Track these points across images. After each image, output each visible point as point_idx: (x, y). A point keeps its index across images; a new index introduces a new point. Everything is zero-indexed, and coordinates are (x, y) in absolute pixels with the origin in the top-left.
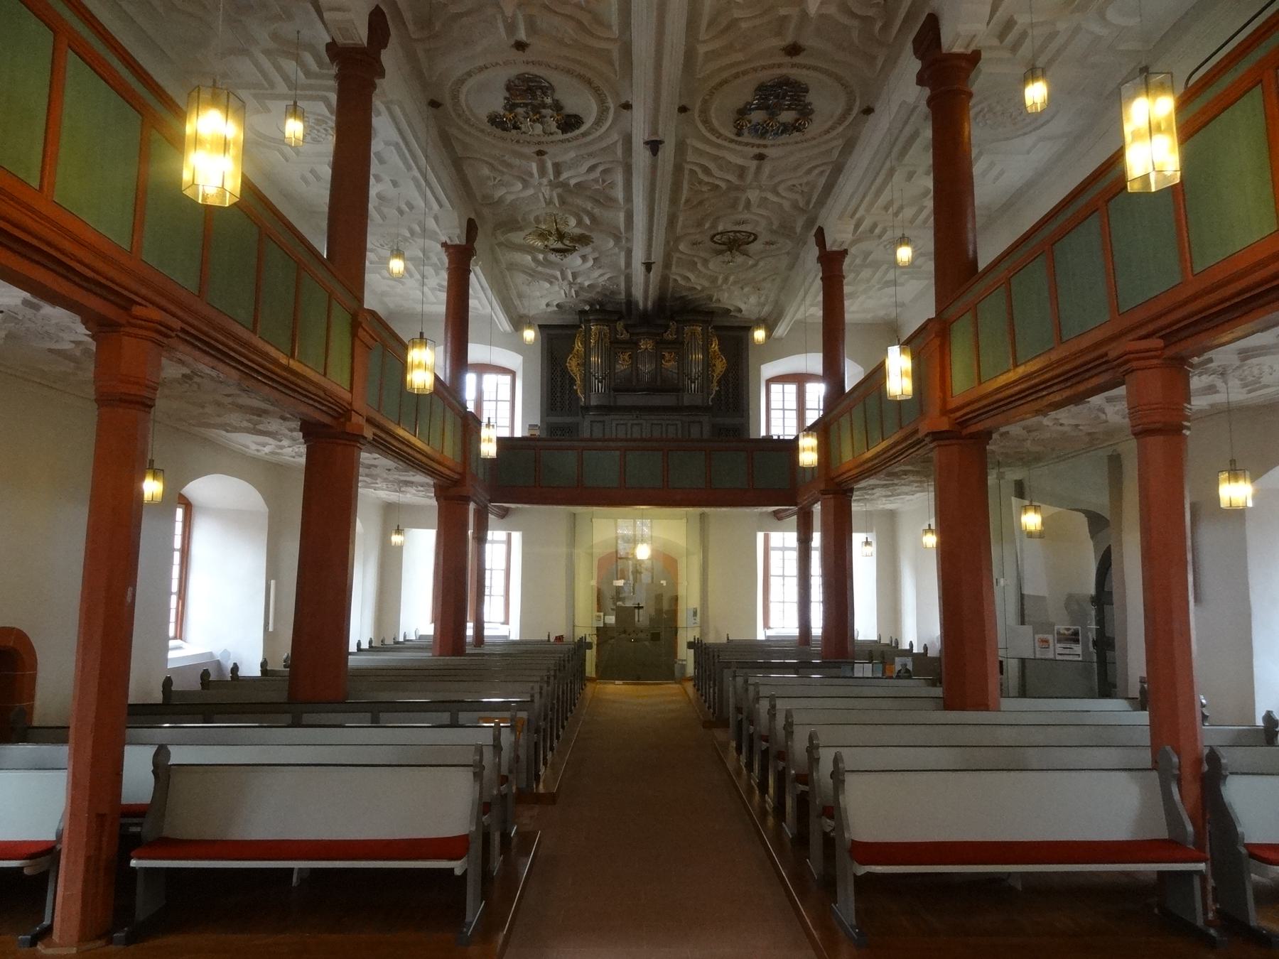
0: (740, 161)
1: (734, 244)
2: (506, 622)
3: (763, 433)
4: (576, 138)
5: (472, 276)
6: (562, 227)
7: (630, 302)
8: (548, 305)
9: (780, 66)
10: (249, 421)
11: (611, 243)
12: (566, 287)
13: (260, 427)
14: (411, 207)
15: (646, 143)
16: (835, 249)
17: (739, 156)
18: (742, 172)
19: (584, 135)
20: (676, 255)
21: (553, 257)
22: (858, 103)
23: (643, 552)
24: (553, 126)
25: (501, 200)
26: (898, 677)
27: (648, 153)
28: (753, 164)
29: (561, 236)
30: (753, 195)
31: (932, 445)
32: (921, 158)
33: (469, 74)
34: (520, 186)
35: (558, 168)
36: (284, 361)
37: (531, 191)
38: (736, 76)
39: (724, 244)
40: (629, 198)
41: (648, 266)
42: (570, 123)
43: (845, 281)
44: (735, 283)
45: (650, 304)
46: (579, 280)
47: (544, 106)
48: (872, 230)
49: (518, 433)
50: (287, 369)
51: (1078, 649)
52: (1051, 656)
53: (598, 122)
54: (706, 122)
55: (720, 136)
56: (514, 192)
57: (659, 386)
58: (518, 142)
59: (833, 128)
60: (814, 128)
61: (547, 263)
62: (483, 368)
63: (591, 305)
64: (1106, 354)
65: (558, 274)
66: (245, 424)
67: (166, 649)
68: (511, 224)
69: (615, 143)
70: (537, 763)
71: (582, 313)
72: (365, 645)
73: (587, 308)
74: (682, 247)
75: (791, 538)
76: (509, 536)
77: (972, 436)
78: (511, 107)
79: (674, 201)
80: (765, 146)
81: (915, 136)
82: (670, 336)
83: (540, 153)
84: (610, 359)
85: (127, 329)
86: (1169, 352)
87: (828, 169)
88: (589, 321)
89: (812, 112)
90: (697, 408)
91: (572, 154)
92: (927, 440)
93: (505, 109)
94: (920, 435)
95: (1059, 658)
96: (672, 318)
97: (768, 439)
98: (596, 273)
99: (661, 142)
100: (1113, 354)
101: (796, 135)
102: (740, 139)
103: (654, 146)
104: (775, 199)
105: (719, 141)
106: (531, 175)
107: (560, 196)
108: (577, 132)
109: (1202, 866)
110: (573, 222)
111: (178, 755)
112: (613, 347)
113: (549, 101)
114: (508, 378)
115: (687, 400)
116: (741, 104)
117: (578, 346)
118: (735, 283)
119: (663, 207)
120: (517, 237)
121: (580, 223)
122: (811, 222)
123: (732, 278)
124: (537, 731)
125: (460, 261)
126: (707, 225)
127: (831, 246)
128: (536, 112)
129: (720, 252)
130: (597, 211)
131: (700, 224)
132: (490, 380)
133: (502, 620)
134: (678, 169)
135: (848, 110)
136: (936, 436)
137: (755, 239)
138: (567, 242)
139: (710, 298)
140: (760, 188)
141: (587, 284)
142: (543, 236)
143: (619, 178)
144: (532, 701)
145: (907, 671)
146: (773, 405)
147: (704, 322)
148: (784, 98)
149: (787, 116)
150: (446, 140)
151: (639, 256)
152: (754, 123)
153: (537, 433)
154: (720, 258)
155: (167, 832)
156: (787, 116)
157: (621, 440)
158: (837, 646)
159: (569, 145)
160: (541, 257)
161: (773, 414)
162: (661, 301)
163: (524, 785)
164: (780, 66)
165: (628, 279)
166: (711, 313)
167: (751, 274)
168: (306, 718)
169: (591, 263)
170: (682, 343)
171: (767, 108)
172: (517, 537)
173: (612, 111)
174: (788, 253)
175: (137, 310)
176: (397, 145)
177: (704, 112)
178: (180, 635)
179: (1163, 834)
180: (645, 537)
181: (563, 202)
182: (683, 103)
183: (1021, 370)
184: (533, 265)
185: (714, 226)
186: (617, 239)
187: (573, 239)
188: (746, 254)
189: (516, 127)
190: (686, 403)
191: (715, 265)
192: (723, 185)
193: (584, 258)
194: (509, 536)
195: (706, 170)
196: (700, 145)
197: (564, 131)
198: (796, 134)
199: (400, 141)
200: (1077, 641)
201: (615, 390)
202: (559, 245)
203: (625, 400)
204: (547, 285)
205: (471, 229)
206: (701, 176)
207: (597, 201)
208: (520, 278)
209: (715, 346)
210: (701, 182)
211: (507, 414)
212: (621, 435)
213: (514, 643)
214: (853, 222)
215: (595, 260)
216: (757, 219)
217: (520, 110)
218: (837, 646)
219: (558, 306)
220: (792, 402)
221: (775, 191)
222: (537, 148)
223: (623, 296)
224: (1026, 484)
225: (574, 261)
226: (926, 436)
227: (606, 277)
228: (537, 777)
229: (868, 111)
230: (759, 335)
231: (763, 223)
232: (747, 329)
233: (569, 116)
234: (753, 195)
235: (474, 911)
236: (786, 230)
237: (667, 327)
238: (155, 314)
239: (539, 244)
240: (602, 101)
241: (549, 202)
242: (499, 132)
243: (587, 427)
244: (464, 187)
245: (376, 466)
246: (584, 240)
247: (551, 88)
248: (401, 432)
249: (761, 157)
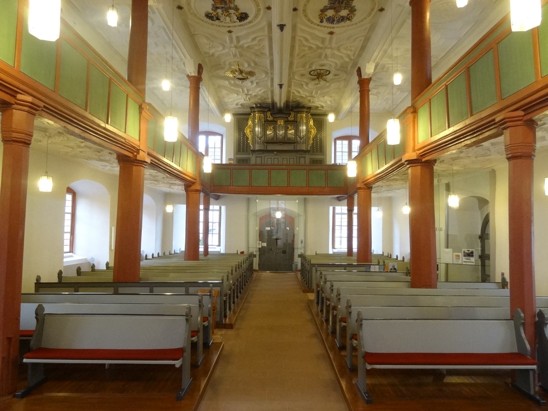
0: (321, 35)
1: (319, 75)
2: (219, 245)
3: (333, 162)
4: (246, 24)
5: (201, 90)
6: (241, 68)
7: (273, 104)
8: (237, 104)
10: (96, 155)
11: (264, 76)
12: (245, 96)
13: (101, 158)
14: (172, 58)
15: (278, 26)
16: (365, 77)
17: (322, 31)
18: (323, 40)
19: (250, 22)
20: (293, 81)
21: (239, 82)
22: (377, 6)
23: (279, 215)
24: (235, 18)
25: (213, 55)
26: (391, 272)
27: (279, 30)
28: (328, 36)
29: (241, 72)
30: (328, 52)
31: (408, 166)
32: (407, 30)
34: (221, 48)
35: (238, 38)
36: (103, 125)
37: (226, 50)
39: (315, 75)
40: (271, 54)
41: (281, 86)
42: (243, 17)
43: (370, 93)
44: (321, 94)
45: (282, 105)
46: (250, 93)
47: (230, 8)
48: (383, 69)
49: (224, 162)
50: (105, 129)
51: (473, 259)
52: (460, 262)
53: (256, 16)
54: (306, 16)
55: (312, 23)
56: (218, 50)
57: (286, 141)
58: (219, 26)
59: (365, 18)
61: (236, 85)
62: (208, 133)
63: (256, 105)
64: (494, 120)
65: (241, 90)
66: (94, 156)
67: (63, 258)
68: (218, 66)
69: (264, 27)
70: (225, 309)
71: (252, 108)
72: (150, 257)
73: (254, 106)
74: (296, 77)
75: (345, 209)
76: (220, 208)
77: (427, 162)
78: (215, 8)
79: (292, 55)
80: (334, 28)
81: (405, 21)
82: (291, 118)
84: (264, 130)
85: (15, 106)
86: (526, 118)
87: (363, 39)
88: (255, 112)
89: (355, 10)
90: (303, 151)
91: (244, 32)
92: (406, 163)
93: (212, 10)
94: (403, 161)
95: (464, 263)
96: (292, 111)
97: (335, 165)
98: (258, 89)
99: (285, 25)
100: (497, 120)
101: (348, 22)
103: (282, 27)
104: (340, 54)
105: (313, 25)
106: (226, 42)
107: (239, 52)
108: (246, 21)
109: (535, 367)
110: (246, 65)
111: (49, 309)
112: (265, 124)
113: (232, 5)
114: (219, 138)
115: (299, 147)
117: (250, 123)
118: (321, 94)
119: (287, 56)
120: (221, 73)
121: (249, 65)
122: (355, 64)
123: (319, 92)
124: (226, 295)
125: (196, 83)
126: (307, 67)
127: (364, 76)
128: (226, 10)
129: (313, 80)
130: (256, 60)
131: (304, 66)
132: (211, 138)
133: (217, 244)
134: (293, 38)
135: (373, 9)
136: (411, 162)
137: (329, 73)
138: (244, 75)
139: (310, 101)
140: (331, 48)
141: (254, 94)
142: (233, 72)
143: (266, 43)
144: (222, 283)
145: (395, 269)
146: (338, 150)
147: (307, 112)
148: (342, 3)
149: (344, 13)
150: (186, 25)
151: (276, 82)
152: (328, 16)
153: (232, 162)
154: (314, 82)
155: (44, 345)
156: (344, 13)
157: (270, 165)
158: (363, 257)
159: (242, 27)
160: (232, 82)
161: (338, 154)
162: (287, 103)
163: (218, 319)
165: (272, 92)
166: (310, 108)
167: (328, 90)
168: (121, 290)
169: (255, 84)
170: (297, 122)
171: (334, 9)
172: (223, 208)
173: (262, 9)
174: (345, 80)
175: (19, 96)
176: (164, 28)
177: (304, 11)
178: (72, 250)
179: (515, 350)
180: (279, 208)
181: (241, 55)
182: (295, 6)
183: (452, 130)
184: (229, 86)
185: (310, 67)
186: (267, 73)
187: (246, 73)
188: (325, 80)
189: (218, 19)
190: (298, 149)
191: (312, 85)
192: (314, 47)
193: (252, 82)
194: (220, 208)
195: (307, 40)
196: (303, 28)
197: (240, 21)
198: (348, 21)
199: (165, 27)
200: (473, 256)
201: (267, 143)
202: (240, 76)
203: (270, 147)
204: (236, 95)
205: (200, 68)
206: (304, 43)
207: (257, 55)
208: (224, 92)
209: (311, 123)
210: (304, 45)
211: (219, 154)
212: (269, 163)
213: (222, 254)
214: (374, 64)
215: (257, 83)
216: (330, 63)
217: (219, 11)
218: (363, 257)
219: (241, 105)
220: (346, 149)
221: (338, 50)
222: (228, 29)
223: (270, 101)
224: (451, 184)
225: (247, 83)
226: (406, 161)
227: (262, 91)
228: (225, 316)
229: (382, 10)
230: (331, 118)
231: (333, 65)
232: (326, 115)
233: (242, 13)
234: (328, 52)
235: (186, 381)
236: (343, 68)
237: (290, 114)
238: (29, 99)
239: (231, 75)
240: (258, 5)
241: (235, 56)
242: (210, 21)
243: (253, 159)
244: (196, 48)
245: (158, 176)
246: (251, 74)
248: (165, 160)
249: (331, 33)
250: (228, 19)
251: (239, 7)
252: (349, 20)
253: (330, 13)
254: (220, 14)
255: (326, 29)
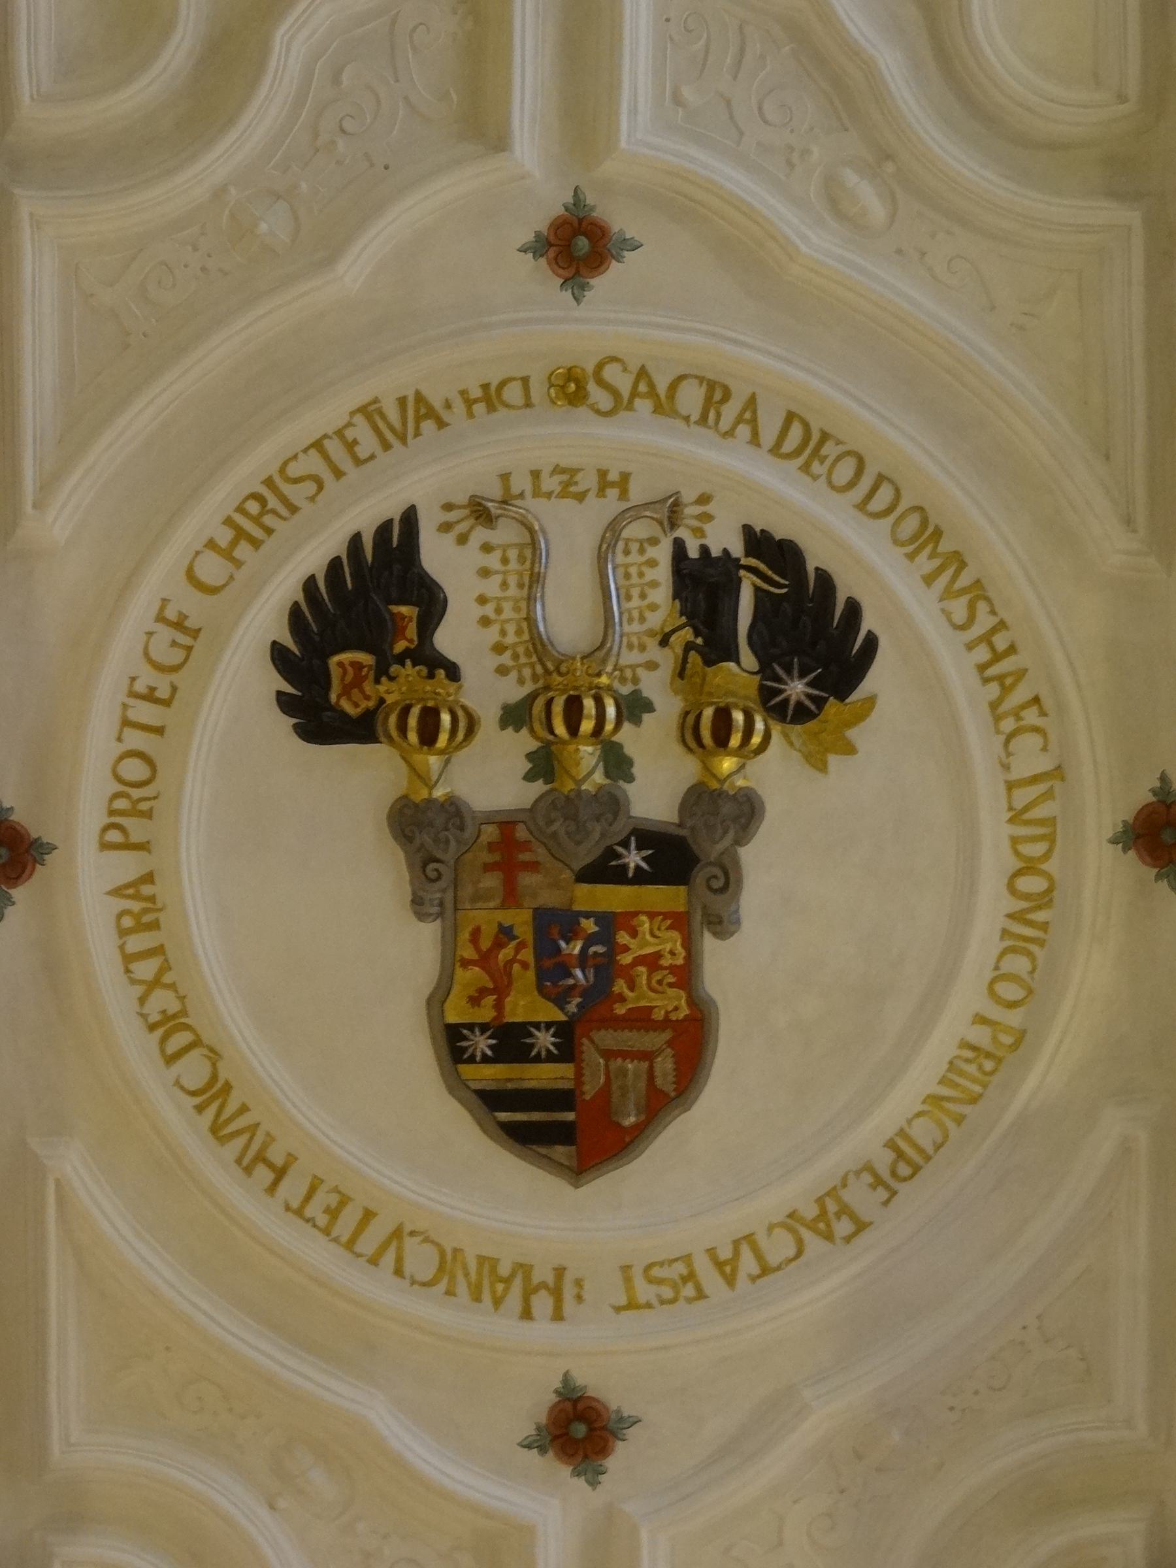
33: (904, 1163)
83: (577, 246)
159: (388, 383)
222: (607, 320)
240: (143, 907)
247: (453, 1043)
250: (568, 619)
251: (384, 872)
254: (667, 706)
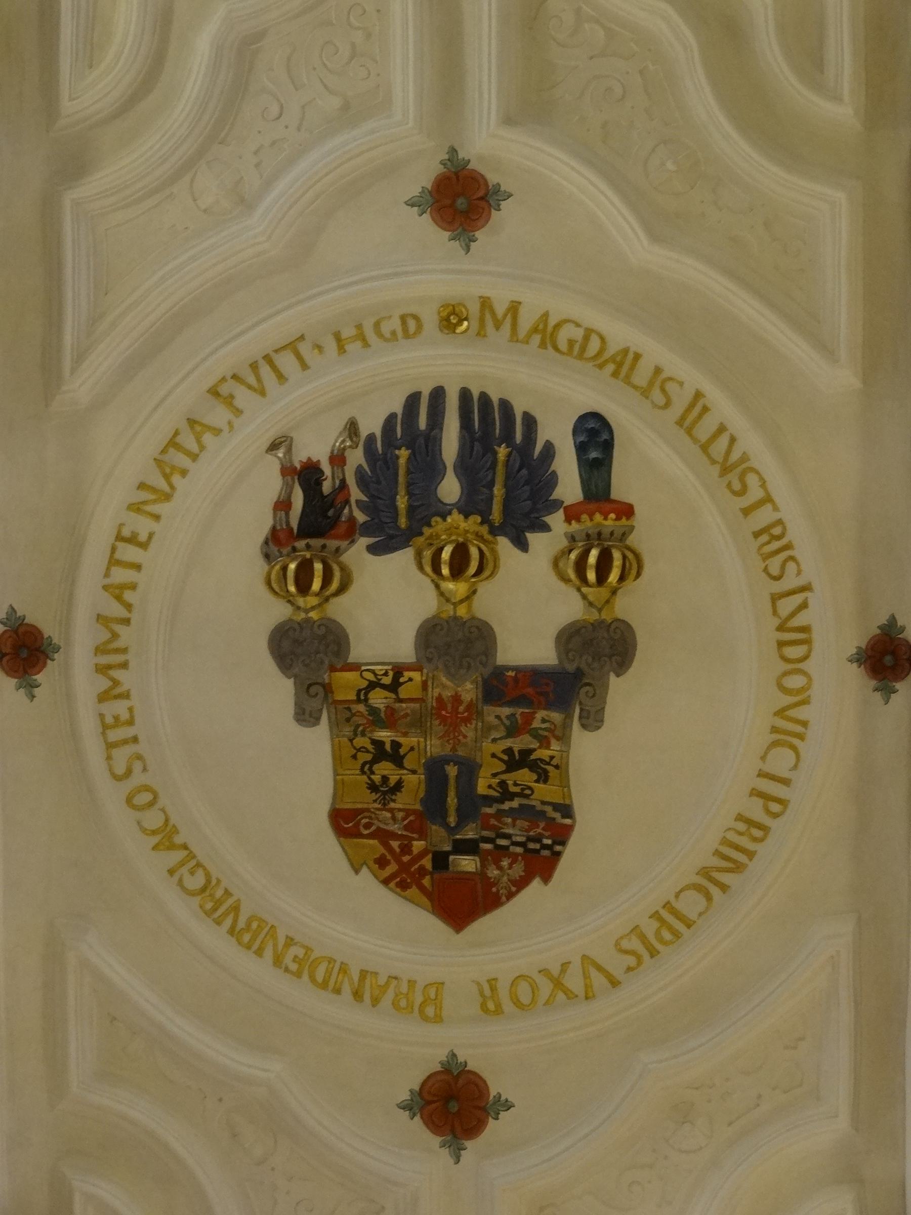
9: (490, 1001)
28: (490, 144)
38: (670, 924)
59: (152, 496)
60: (238, 495)
102: (584, 392)
105: (689, 375)
116: (620, 691)
164: (490, 1001)
177: (793, 637)
198: (315, 447)
252: (309, 475)
253: (528, 603)
255: (536, 302)
